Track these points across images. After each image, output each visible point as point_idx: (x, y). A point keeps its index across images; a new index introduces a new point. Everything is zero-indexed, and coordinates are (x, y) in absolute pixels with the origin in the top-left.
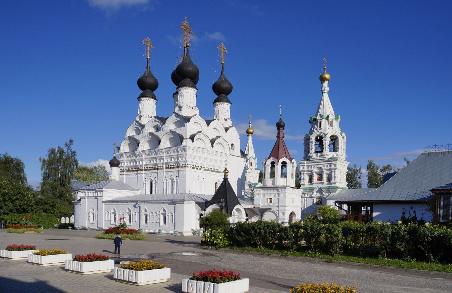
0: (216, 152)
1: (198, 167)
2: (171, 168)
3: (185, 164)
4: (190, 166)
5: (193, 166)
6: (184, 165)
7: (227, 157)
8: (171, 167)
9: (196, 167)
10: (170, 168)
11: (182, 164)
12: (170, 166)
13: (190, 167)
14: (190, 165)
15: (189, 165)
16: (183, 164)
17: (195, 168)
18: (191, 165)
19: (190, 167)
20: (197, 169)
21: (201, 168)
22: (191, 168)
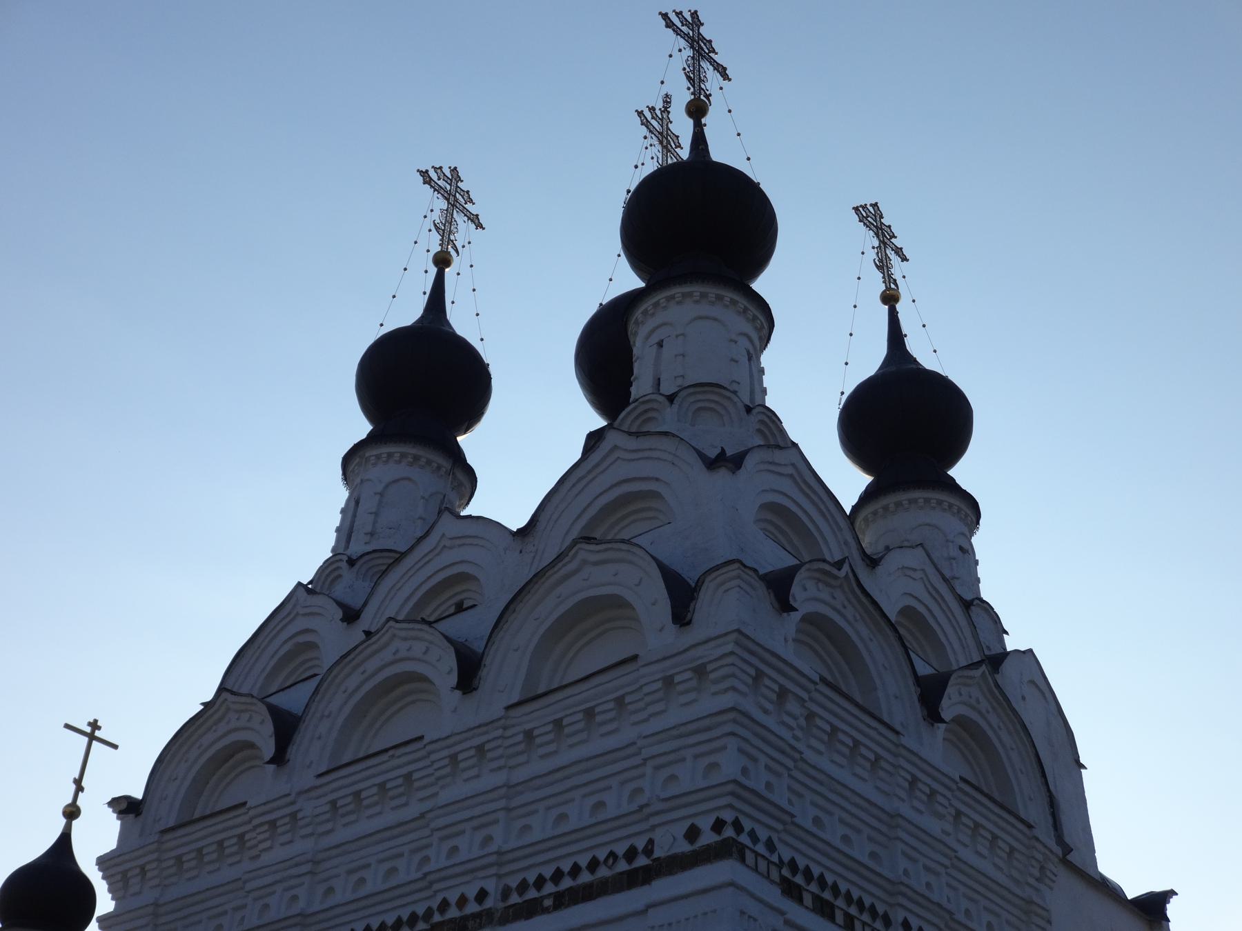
0: (963, 785)
1: (827, 895)
2: (562, 901)
3: (718, 826)
4: (767, 854)
5: (786, 872)
6: (708, 838)
7: (1042, 868)
8: (567, 883)
9: (814, 887)
10: (548, 903)
11: (683, 827)
12: (558, 876)
13: (762, 865)
14: (760, 848)
15: (753, 835)
16: (692, 833)
17: (808, 899)
18: (770, 845)
19: (762, 865)
20: (824, 909)
21: (853, 911)
22: (775, 875)
